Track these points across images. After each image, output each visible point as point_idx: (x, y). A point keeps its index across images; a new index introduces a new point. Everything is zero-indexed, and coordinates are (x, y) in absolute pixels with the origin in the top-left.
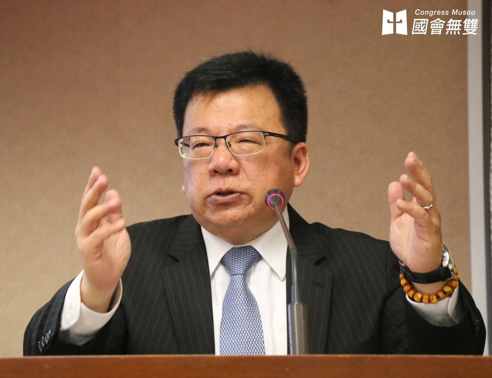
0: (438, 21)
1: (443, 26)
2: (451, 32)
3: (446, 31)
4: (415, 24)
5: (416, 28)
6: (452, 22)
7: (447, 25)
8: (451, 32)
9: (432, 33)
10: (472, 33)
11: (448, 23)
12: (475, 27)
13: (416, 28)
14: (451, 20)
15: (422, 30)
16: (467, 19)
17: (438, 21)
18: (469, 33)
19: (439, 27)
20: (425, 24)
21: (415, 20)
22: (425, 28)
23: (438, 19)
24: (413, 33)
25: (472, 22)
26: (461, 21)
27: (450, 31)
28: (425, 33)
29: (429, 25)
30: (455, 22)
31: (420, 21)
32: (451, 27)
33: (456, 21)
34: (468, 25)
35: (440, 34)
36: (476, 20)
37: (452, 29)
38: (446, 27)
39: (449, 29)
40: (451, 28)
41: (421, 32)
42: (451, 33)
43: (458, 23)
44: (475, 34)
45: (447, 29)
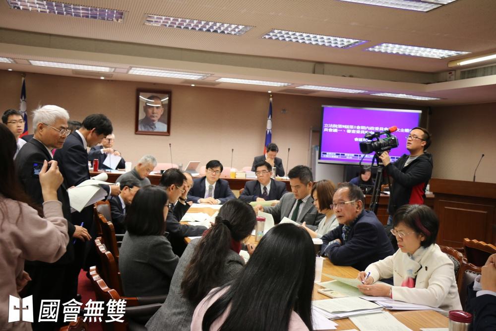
0: (73, 302)
1: (79, 310)
2: (90, 318)
3: (85, 317)
4: (43, 307)
5: (44, 312)
6: (91, 305)
7: (85, 309)
8: (90, 318)
9: (65, 321)
10: (117, 320)
11: (86, 305)
12: (121, 312)
13: (44, 312)
14: (90, 302)
15: (51, 315)
16: (111, 300)
17: (73, 302)
18: (114, 320)
19: (75, 311)
20: (56, 307)
21: (43, 301)
22: (55, 313)
23: (74, 300)
24: (40, 320)
25: (118, 304)
26: (103, 302)
27: (88, 317)
28: (56, 320)
29: (62, 308)
30: (95, 305)
31: (49, 303)
32: (91, 311)
33: (97, 303)
34: (113, 309)
35: (75, 321)
36: (124, 302)
37: (92, 314)
38: (83, 312)
39: (88, 314)
40: (90, 313)
41: (51, 318)
42: (90, 321)
43: (99, 305)
44: (122, 321)
45: (85, 315)
